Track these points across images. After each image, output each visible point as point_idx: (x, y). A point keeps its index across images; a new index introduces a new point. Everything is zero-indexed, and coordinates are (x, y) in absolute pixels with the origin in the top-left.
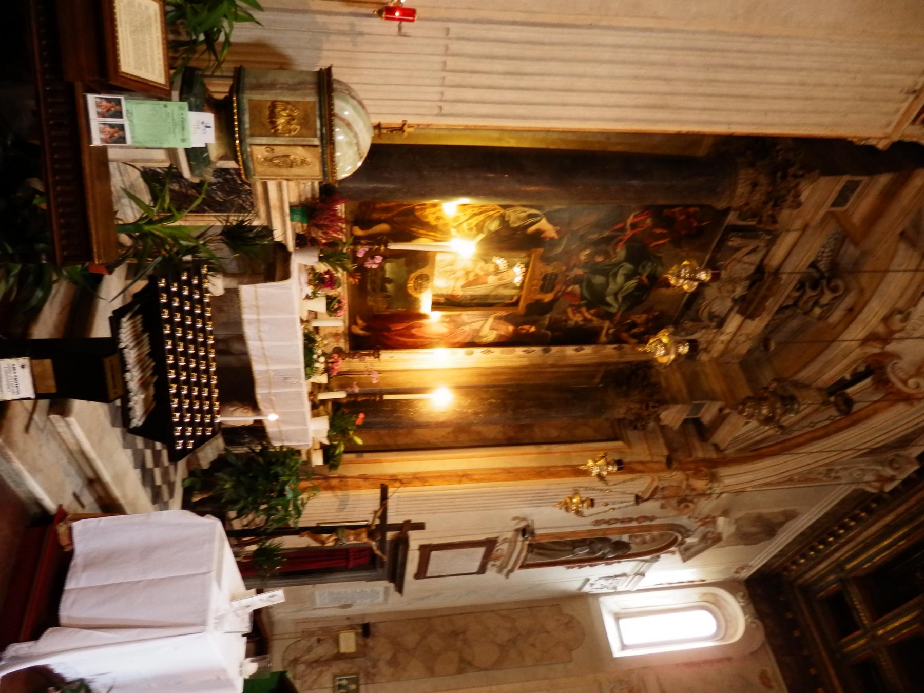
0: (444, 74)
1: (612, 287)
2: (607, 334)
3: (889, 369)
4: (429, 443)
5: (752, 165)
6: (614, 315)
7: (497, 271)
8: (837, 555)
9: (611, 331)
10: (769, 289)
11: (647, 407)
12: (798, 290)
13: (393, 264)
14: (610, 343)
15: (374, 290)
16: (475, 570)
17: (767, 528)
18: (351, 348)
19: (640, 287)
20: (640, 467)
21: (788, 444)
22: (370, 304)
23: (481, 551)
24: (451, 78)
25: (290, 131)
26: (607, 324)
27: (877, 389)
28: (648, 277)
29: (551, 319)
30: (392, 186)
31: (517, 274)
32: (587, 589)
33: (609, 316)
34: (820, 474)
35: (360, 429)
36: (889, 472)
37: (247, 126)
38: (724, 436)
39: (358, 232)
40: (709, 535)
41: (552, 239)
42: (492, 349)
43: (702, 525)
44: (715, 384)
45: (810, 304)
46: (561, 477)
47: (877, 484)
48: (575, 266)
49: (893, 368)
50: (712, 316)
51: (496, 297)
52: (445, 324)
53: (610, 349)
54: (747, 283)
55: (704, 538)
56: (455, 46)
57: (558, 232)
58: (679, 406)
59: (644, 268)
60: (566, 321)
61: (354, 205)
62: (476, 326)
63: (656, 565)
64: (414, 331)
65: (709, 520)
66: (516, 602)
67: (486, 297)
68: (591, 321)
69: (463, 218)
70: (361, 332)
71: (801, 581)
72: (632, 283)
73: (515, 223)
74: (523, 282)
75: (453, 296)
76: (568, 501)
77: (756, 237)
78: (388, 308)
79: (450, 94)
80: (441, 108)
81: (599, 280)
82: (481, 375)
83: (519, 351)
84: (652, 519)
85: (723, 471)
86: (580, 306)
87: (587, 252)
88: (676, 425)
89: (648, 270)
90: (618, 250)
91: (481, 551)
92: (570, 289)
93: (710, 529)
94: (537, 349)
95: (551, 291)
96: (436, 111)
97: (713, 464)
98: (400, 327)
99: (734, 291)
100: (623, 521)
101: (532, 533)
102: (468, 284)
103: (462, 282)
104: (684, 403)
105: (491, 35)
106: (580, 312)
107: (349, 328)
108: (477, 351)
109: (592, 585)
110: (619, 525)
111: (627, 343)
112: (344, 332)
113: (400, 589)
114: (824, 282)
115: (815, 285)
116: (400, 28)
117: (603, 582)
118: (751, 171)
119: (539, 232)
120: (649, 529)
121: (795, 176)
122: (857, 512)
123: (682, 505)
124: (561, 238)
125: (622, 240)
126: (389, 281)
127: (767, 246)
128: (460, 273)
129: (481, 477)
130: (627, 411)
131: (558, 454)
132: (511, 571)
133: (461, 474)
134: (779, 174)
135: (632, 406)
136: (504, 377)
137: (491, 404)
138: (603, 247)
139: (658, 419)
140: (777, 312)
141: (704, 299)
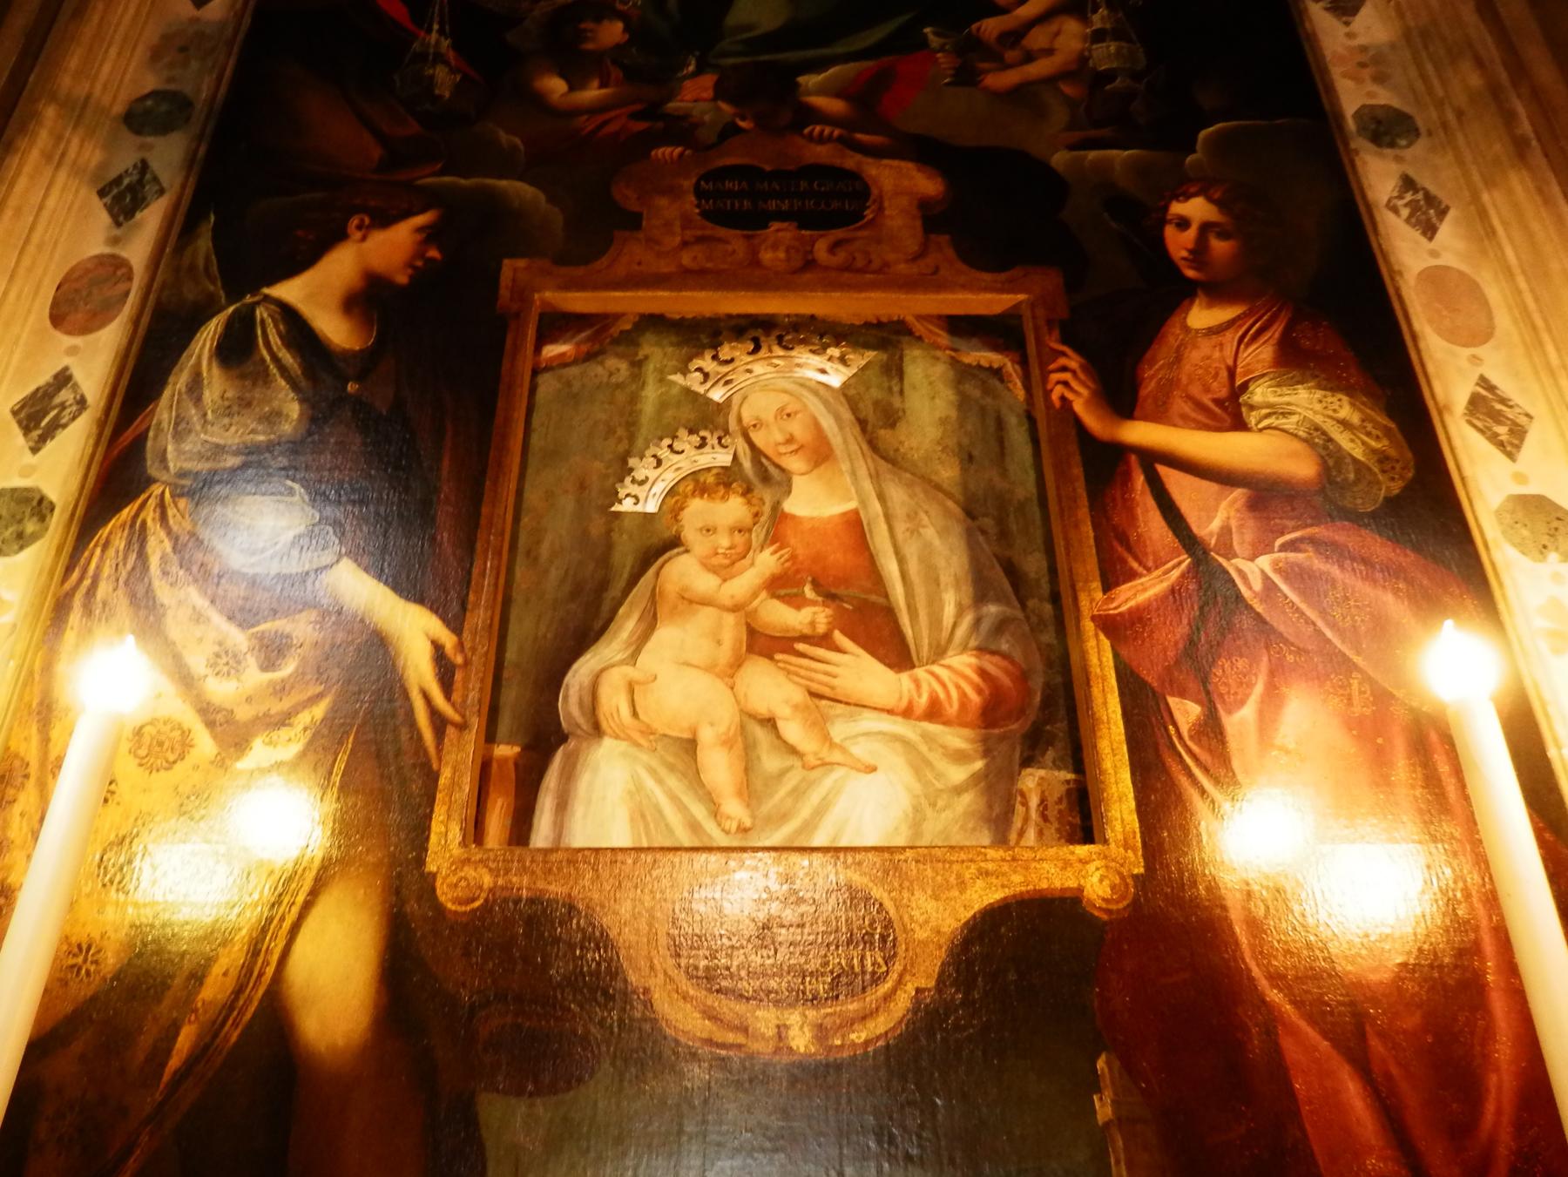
48: (652, 111)
52: (1240, 721)
57: (384, 220)
75: (992, 713)
103: (859, 671)
128: (769, 688)
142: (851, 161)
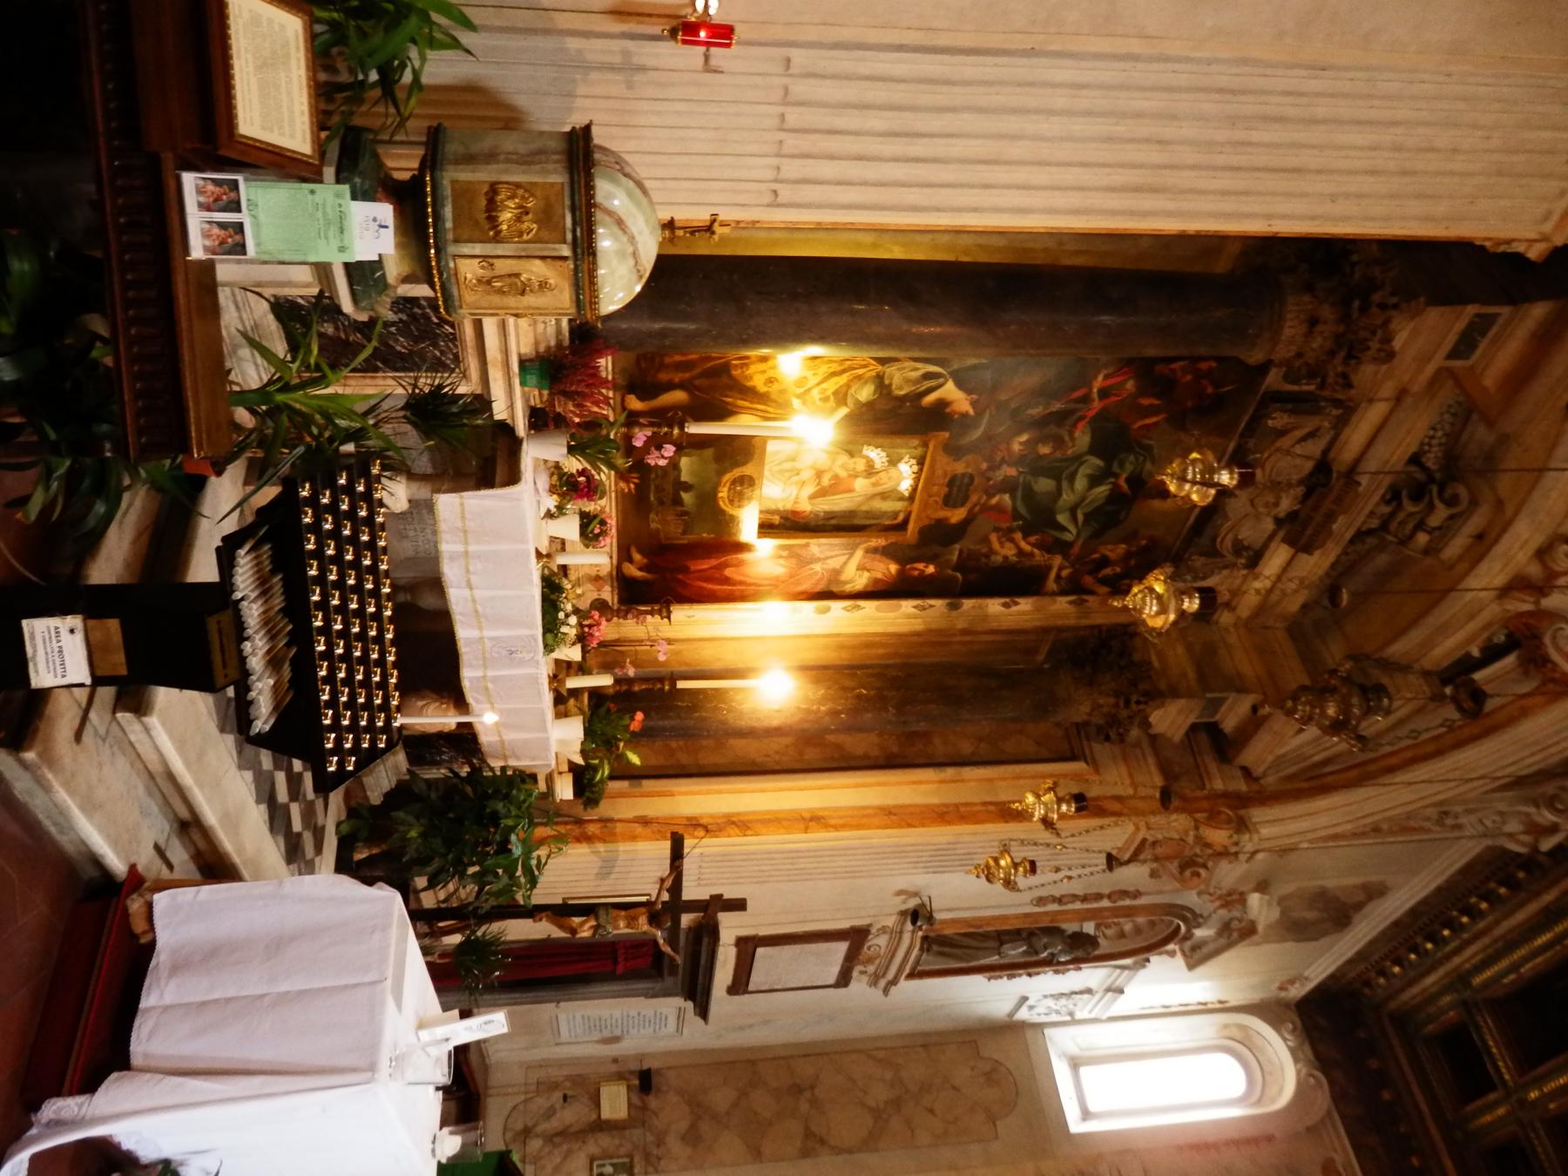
0: (782, 135)
1: (1067, 498)
2: (1058, 577)
3: (1547, 640)
4: (754, 763)
5: (1309, 288)
6: (1070, 545)
7: (870, 471)
8: (1457, 960)
9: (1065, 573)
10: (1339, 500)
11: (1127, 703)
12: (1388, 503)
13: (694, 458)
14: (1063, 593)
15: (661, 503)
16: (832, 980)
17: (1336, 913)
18: (621, 601)
19: (1115, 497)
20: (1117, 806)
21: (1372, 768)
22: (653, 526)
23: (842, 948)
24: (792, 143)
25: (521, 234)
26: (1057, 560)
27: (1526, 673)
28: (1128, 480)
29: (961, 552)
30: (693, 327)
31: (905, 476)
32: (1023, 1014)
33: (1063, 547)
34: (1428, 819)
35: (636, 739)
36: (1548, 817)
37: (449, 225)
38: (1258, 753)
39: (635, 404)
40: (1235, 924)
41: (965, 415)
42: (862, 603)
43: (1222, 906)
44: (1244, 663)
45: (1410, 526)
46: (977, 823)
47: (1527, 838)
48: (1003, 461)
49: (1554, 638)
50: (1239, 548)
51: (869, 514)
52: (782, 561)
53: (1063, 604)
54: (1300, 490)
55: (1225, 928)
56: (800, 89)
57: (974, 404)
58: (1182, 702)
59: (1122, 465)
60: (987, 556)
61: (628, 358)
62: (834, 563)
63: (1142, 974)
64: (728, 572)
65: (1235, 899)
66: (902, 1036)
67: (851, 514)
68: (1032, 555)
69: (813, 381)
70: (638, 574)
71: (1393, 1005)
72: (1102, 490)
73: (900, 388)
74: (915, 489)
75: (794, 513)
76: (992, 863)
77: (1317, 411)
78: (684, 533)
79: (791, 169)
80: (775, 192)
81: (1044, 485)
82: (842, 647)
83: (908, 606)
84: (1137, 894)
85: (1257, 814)
86: (1011, 530)
87: (1024, 438)
88: (1178, 735)
89: (1129, 468)
90: (1077, 434)
91: (842, 948)
92: (994, 501)
93: (1236, 913)
94: (939, 604)
95: (963, 505)
96: (768, 199)
97: (1241, 801)
98: (705, 565)
99: (1276, 504)
100: (1085, 899)
101: (930, 918)
102: (822, 493)
103: (810, 489)
104: (1190, 695)
105: (863, 69)
106: (1012, 540)
107: (619, 568)
108: (837, 606)
109: (1031, 1008)
110: (1078, 905)
111: (1092, 593)
112: (610, 574)
113: (703, 1011)
114: (1435, 489)
115: (1418, 494)
116: (707, 57)
117: (1050, 1003)
118: (1307, 298)
119: (942, 404)
120: (1129, 912)
121: (1383, 307)
122: (1492, 885)
123: (1188, 873)
124: (979, 414)
125: (1081, 418)
126: (687, 487)
127: (1335, 427)
128: (807, 474)
129: (841, 822)
130: (1093, 710)
131: (972, 784)
132: (894, 982)
133: (807, 815)
134: (1356, 304)
135: (1101, 701)
136: (881, 651)
137: (859, 697)
138: (1052, 429)
139: (1145, 725)
140: (1352, 541)
141: (1226, 518)
142: (968, 505)
